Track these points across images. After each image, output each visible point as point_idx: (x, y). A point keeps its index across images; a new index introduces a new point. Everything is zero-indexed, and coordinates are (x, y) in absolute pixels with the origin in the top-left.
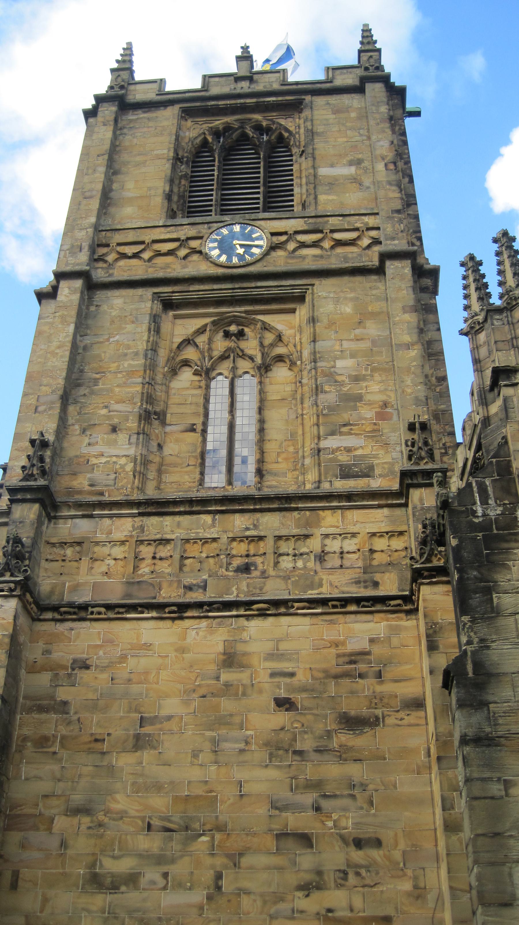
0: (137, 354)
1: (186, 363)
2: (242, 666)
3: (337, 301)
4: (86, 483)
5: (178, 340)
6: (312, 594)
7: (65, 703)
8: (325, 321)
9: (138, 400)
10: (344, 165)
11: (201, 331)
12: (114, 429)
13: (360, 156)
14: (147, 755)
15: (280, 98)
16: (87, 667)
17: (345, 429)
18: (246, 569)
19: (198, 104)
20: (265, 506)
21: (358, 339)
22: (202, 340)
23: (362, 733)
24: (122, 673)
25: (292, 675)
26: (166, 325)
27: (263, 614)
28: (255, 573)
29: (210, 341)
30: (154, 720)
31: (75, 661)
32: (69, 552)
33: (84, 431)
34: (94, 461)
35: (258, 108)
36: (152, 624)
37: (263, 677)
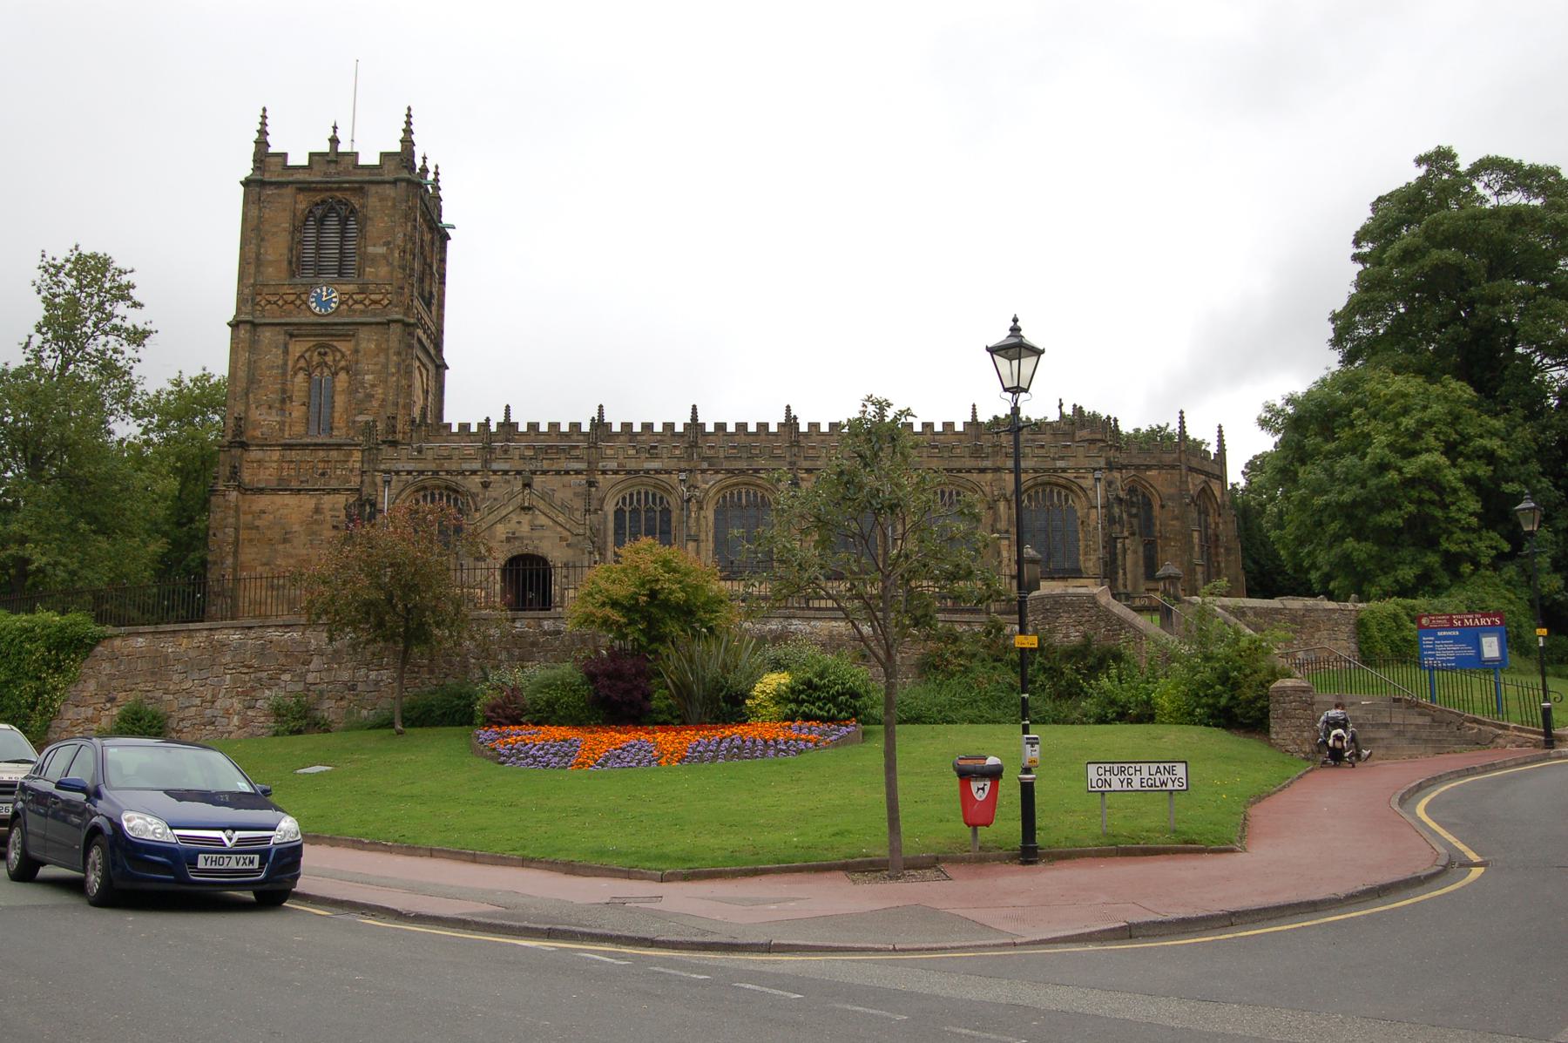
2: (321, 513)
3: (368, 340)
5: (298, 355)
6: (347, 486)
8: (362, 352)
11: (306, 351)
12: (270, 408)
14: (288, 545)
18: (323, 474)
19: (305, 185)
21: (375, 364)
24: (278, 514)
26: (291, 348)
27: (329, 493)
30: (290, 532)
35: (338, 189)
37: (328, 518)
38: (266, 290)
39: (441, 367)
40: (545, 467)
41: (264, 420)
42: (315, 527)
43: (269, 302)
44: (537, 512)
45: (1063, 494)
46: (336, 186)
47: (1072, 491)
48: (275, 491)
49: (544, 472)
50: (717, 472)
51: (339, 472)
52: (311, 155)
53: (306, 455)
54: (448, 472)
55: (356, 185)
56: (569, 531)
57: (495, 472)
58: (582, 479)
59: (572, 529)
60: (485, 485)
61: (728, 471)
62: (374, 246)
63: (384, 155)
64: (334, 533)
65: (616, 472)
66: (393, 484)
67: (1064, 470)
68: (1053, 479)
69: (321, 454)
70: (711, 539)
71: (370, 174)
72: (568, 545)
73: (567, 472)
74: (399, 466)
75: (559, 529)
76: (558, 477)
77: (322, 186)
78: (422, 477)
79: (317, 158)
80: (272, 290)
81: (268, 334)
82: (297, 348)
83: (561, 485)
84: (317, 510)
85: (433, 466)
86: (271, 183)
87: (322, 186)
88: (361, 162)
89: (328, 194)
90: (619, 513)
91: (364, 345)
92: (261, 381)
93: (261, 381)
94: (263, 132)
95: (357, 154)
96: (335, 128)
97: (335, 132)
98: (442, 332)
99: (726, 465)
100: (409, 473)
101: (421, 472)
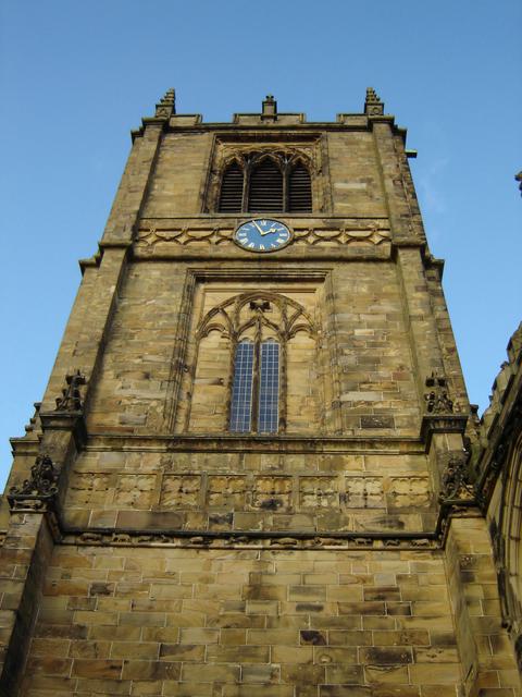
0: (171, 315)
1: (215, 327)
2: (268, 598)
4: (117, 421)
5: (207, 309)
7: (82, 628)
8: (344, 298)
9: (171, 353)
10: (356, 182)
11: (228, 303)
12: (147, 376)
13: (370, 176)
16: (108, 593)
17: (363, 386)
18: (271, 505)
20: (290, 447)
21: (374, 313)
22: (229, 309)
23: (393, 670)
24: (144, 599)
25: (319, 608)
26: (199, 298)
27: (289, 548)
29: (238, 311)
30: (173, 650)
31: (95, 586)
32: (96, 482)
33: (118, 377)
34: (126, 402)
36: (176, 551)
37: (289, 611)
42: (251, 636)
51: (311, 501)
64: (308, 652)
69: (265, 462)
81: (156, 274)
82: (211, 297)
84: (257, 591)
91: (344, 288)
92: (132, 336)
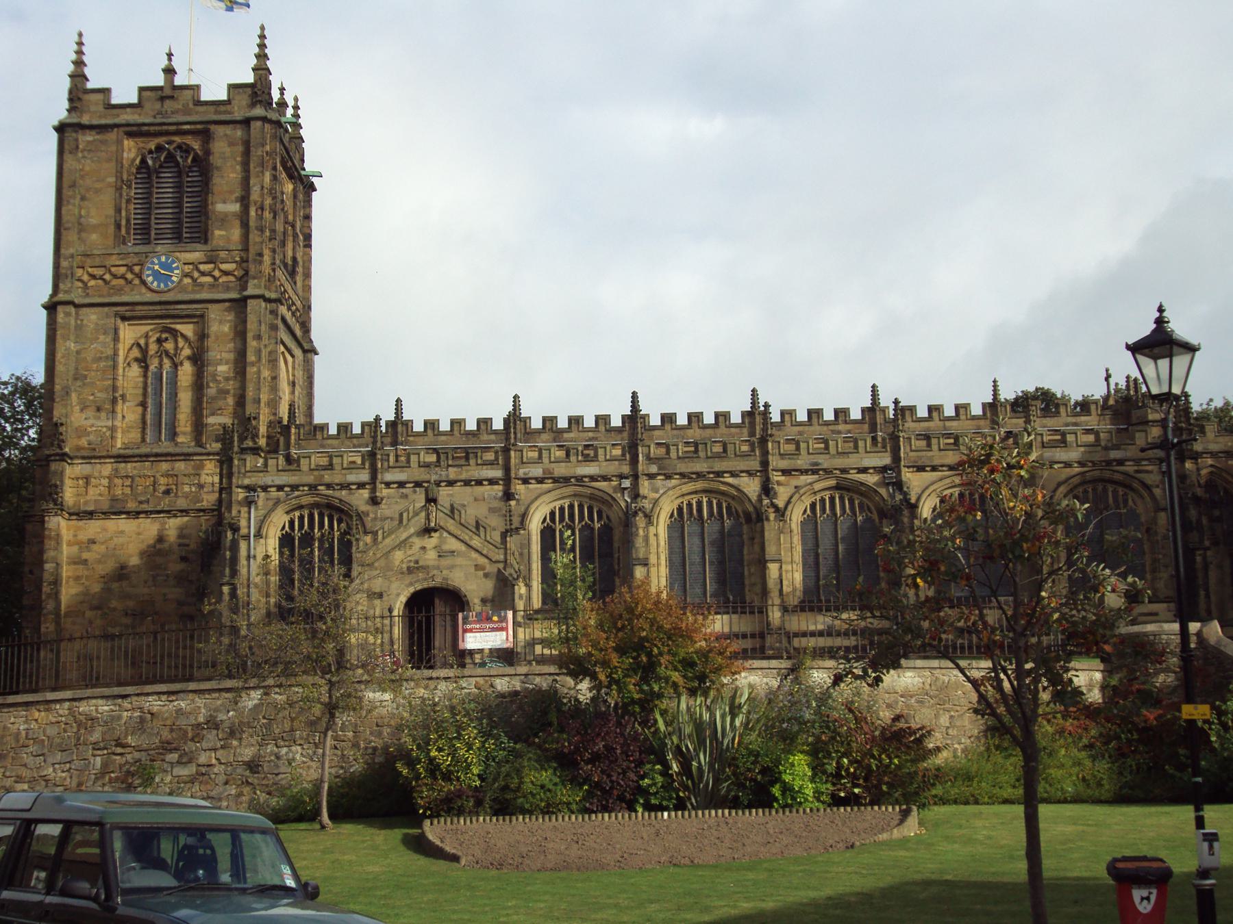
3: (221, 322)
6: (198, 505)
7: (86, 560)
10: (232, 202)
12: (99, 409)
14: (125, 583)
15: (193, 127)
16: (95, 543)
17: (219, 412)
18: (167, 492)
19: (135, 129)
20: (177, 458)
24: (111, 545)
25: (188, 545)
27: (175, 516)
28: (172, 495)
31: (89, 540)
33: (82, 410)
34: (89, 429)
36: (124, 521)
38: (89, 261)
39: (310, 351)
40: (452, 476)
41: (92, 426)
43: (93, 277)
44: (445, 534)
45: (1121, 493)
46: (174, 128)
47: (1132, 489)
48: (107, 514)
49: (451, 483)
50: (668, 477)
51: (187, 489)
52: (142, 90)
53: (146, 468)
54: (329, 486)
55: (199, 127)
56: (486, 557)
57: (388, 485)
58: (498, 489)
59: (491, 555)
60: (374, 501)
61: (683, 475)
62: (224, 202)
63: (233, 88)
65: (540, 481)
66: (260, 503)
67: (1120, 462)
68: (1107, 474)
69: (164, 466)
70: (663, 562)
71: (216, 112)
72: (486, 576)
73: (479, 483)
74: (268, 479)
75: (474, 555)
76: (468, 489)
77: (157, 128)
78: (297, 493)
79: (148, 93)
80: (97, 261)
82: (129, 333)
83: (472, 499)
85: (310, 479)
86: (91, 127)
87: (157, 128)
88: (205, 96)
89: (165, 139)
90: (548, 534)
92: (85, 377)
93: (85, 377)
94: (79, 63)
95: (198, 87)
96: (170, 55)
97: (170, 60)
98: (310, 307)
99: (683, 467)
100: (280, 488)
101: (294, 487)
